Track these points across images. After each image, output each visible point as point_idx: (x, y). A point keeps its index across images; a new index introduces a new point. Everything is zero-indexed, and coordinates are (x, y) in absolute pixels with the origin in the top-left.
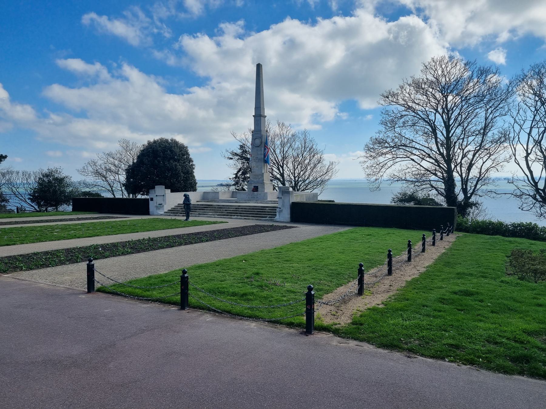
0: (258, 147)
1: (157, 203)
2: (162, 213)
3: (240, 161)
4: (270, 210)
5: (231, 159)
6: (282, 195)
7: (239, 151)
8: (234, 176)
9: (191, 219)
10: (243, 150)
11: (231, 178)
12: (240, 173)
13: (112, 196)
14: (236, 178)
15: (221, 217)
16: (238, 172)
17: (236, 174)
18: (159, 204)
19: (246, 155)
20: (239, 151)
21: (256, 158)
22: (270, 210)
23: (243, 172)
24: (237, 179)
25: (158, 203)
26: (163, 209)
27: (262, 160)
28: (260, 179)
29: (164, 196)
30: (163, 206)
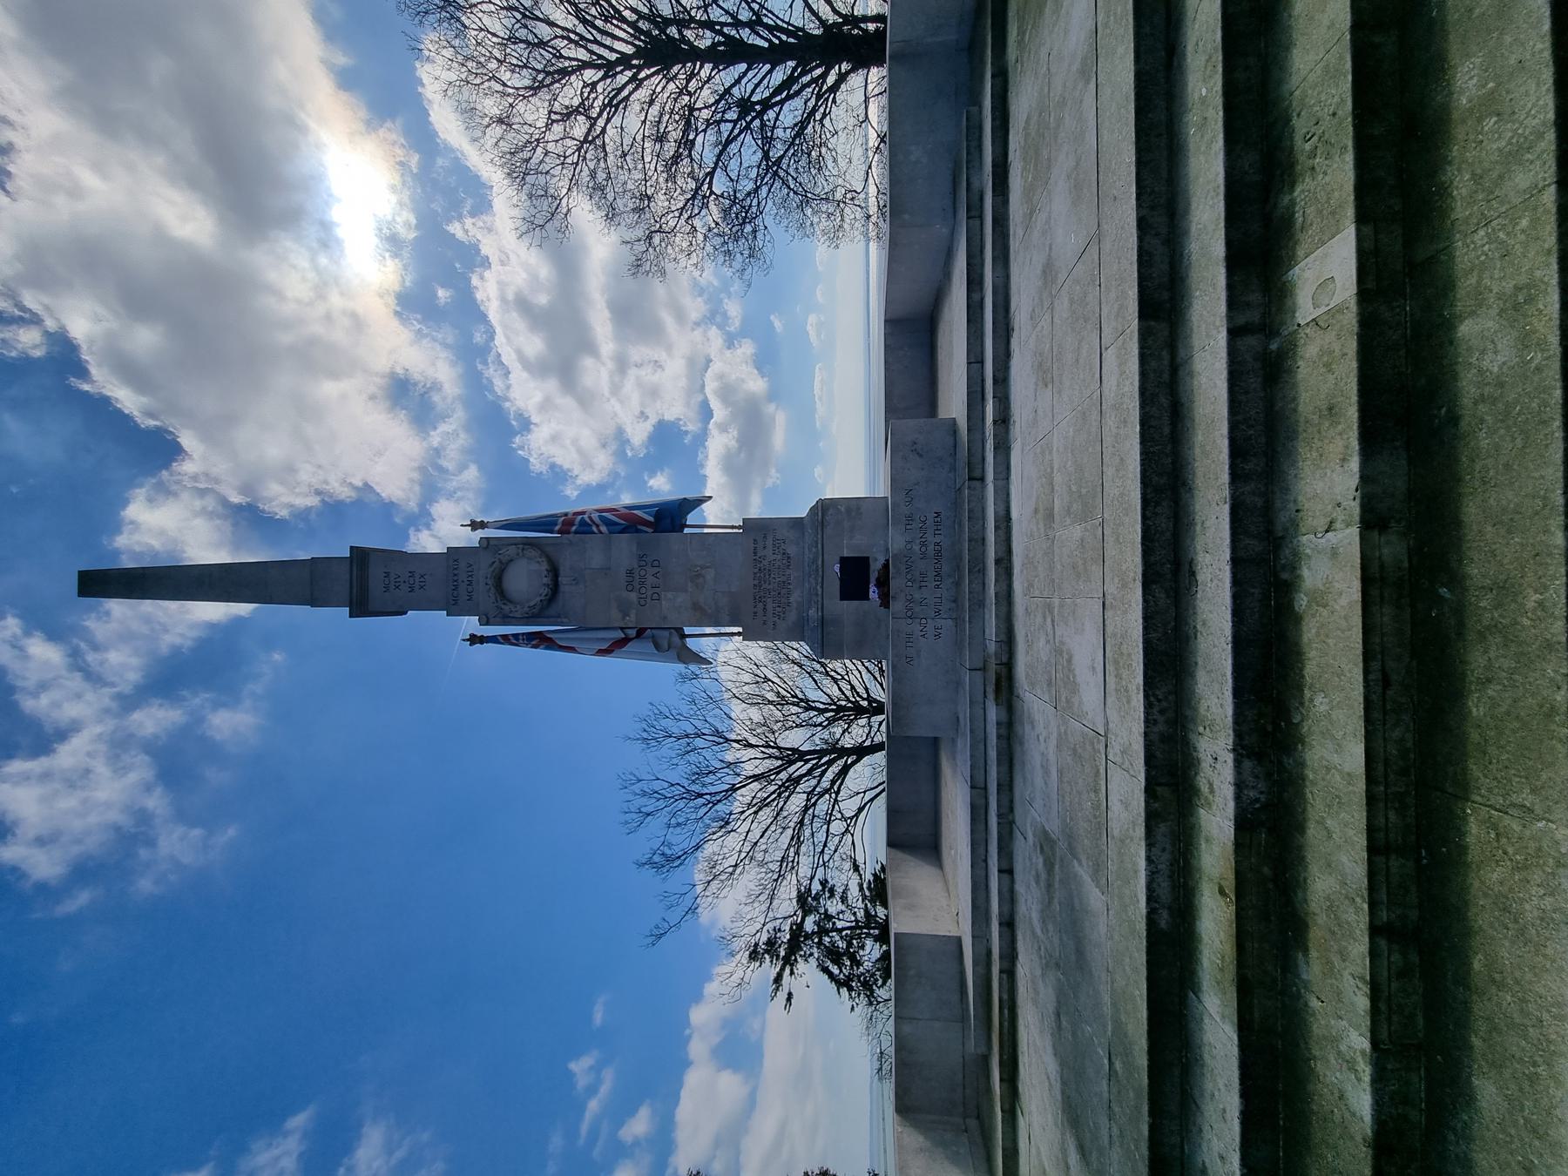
0: (554, 572)
3: (801, 966)
5: (790, 996)
7: (769, 969)
8: (844, 991)
10: (766, 951)
11: (850, 1004)
14: (850, 989)
17: (840, 984)
19: (780, 946)
21: (630, 587)
24: (854, 984)
28: (792, 550)
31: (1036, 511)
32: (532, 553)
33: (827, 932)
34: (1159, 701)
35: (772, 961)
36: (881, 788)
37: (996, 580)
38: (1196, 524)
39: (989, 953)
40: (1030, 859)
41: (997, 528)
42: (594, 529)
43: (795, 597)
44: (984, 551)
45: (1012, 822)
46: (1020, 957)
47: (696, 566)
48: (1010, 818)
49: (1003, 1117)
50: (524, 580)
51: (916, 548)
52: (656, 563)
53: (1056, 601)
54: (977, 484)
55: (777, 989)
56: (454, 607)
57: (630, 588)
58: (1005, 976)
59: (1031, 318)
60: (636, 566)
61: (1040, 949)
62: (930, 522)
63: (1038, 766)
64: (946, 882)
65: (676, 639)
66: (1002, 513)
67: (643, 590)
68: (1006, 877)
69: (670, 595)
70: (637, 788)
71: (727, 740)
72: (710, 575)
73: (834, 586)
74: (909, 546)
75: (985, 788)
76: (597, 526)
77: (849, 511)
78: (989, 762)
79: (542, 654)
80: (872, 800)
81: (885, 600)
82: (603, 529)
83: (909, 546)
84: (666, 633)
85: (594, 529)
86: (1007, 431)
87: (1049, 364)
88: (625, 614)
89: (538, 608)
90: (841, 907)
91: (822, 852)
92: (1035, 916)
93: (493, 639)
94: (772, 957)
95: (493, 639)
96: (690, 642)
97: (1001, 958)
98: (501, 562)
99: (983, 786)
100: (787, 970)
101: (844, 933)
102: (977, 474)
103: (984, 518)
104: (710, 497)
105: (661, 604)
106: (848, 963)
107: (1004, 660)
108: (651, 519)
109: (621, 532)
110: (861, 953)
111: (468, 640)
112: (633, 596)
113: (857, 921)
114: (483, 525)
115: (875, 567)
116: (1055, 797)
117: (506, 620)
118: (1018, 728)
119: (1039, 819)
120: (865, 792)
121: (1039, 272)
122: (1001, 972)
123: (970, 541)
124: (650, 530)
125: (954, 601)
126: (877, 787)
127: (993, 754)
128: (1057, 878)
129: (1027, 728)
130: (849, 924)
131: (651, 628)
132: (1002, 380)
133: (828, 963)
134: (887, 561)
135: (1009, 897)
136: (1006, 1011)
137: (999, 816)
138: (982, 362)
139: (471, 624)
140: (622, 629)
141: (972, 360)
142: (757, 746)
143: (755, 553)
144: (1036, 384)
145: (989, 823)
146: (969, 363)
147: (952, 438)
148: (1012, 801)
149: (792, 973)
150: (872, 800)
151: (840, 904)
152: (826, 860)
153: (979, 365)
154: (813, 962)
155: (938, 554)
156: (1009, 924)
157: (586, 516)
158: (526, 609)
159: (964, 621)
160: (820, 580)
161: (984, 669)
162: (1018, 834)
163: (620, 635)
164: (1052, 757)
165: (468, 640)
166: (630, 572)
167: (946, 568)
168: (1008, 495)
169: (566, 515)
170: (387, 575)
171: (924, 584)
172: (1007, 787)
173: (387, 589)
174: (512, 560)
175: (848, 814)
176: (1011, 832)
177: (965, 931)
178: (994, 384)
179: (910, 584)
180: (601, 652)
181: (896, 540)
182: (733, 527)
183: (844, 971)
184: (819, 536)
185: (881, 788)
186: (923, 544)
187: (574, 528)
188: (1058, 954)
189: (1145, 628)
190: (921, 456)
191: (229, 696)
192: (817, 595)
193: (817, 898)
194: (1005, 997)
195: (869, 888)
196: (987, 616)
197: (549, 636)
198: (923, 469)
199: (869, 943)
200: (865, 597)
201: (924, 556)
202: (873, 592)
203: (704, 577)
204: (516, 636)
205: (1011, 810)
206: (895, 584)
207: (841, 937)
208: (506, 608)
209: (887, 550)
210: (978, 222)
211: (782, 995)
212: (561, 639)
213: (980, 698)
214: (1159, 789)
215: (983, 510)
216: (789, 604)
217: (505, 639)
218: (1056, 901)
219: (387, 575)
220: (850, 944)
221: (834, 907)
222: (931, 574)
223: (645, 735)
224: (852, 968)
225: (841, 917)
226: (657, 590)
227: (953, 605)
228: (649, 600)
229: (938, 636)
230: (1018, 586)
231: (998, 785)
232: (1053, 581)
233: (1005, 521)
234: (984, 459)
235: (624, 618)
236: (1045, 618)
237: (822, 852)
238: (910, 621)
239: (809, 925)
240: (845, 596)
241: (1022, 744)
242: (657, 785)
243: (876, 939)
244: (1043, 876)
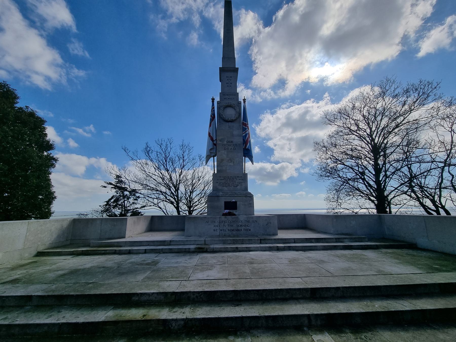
0: (232, 121)
3: (114, 190)
5: (105, 187)
7: (114, 181)
8: (106, 203)
10: (119, 180)
12: (112, 201)
14: (106, 205)
17: (108, 202)
19: (120, 184)
20: (114, 181)
21: (228, 142)
24: (108, 206)
28: (239, 187)
31: (253, 259)
32: (237, 115)
33: (124, 198)
34: (200, 296)
35: (116, 182)
36: (167, 214)
37: (231, 247)
38: (252, 306)
39: (121, 246)
40: (149, 259)
41: (247, 247)
42: (244, 132)
43: (225, 188)
44: (240, 244)
45: (160, 253)
46: (120, 256)
47: (234, 160)
48: (161, 253)
49: (71, 251)
50: (230, 113)
51: (240, 224)
52: (235, 149)
53: (227, 265)
54: (259, 242)
55: (107, 183)
56: (222, 95)
57: (228, 142)
58: (114, 251)
59: (308, 257)
60: (234, 143)
61: (123, 262)
62: (248, 228)
63: (178, 261)
64: (141, 233)
65: (213, 155)
66: (251, 249)
67: (227, 145)
68: (144, 251)
69: (226, 153)
70: (168, 143)
71: (182, 169)
73: (228, 200)
74: (240, 221)
75: (170, 245)
76: (245, 133)
77: (250, 204)
78: (178, 246)
79: (209, 118)
80: (163, 211)
81: (225, 215)
82: (244, 134)
83: (240, 221)
84: (215, 152)
85: (244, 132)
86: (275, 250)
87: (296, 262)
88: (220, 141)
89: (222, 117)
90: (131, 202)
91: (148, 197)
92: (133, 260)
93: (213, 104)
94: (117, 182)
95: (213, 104)
96: (212, 158)
97: (120, 250)
98: (235, 107)
99: (171, 244)
100: (113, 186)
101: (123, 203)
102: (262, 242)
103: (249, 244)
104: (253, 164)
105: (223, 150)
106: (114, 205)
107: (208, 250)
108: (247, 148)
109: (243, 139)
111: (213, 98)
112: (225, 143)
113: (127, 207)
114: (244, 102)
115: (234, 212)
116: (169, 266)
117: (219, 108)
118: (188, 254)
119: (162, 261)
120: (165, 209)
121: (322, 259)
122: (115, 250)
123: (243, 240)
124: (244, 147)
125: (224, 235)
126: (167, 213)
127: (180, 247)
128: (145, 267)
129: (189, 257)
130: (126, 204)
131: (216, 148)
132: (290, 249)
133: (114, 199)
134: (236, 215)
135: (137, 253)
136: (103, 252)
137: (162, 249)
138: (295, 243)
139: (217, 99)
140: (216, 140)
141: (295, 240)
142: (180, 177)
143: (238, 177)
144: (289, 259)
145: (160, 246)
146: (294, 239)
147: (272, 234)
148: (166, 253)
149: (112, 188)
150: (163, 211)
151: (132, 202)
152: (146, 198)
153: (294, 242)
154: (115, 194)
155: (238, 230)
156: (129, 252)
157: (247, 130)
158: (222, 114)
159: (219, 238)
160: (230, 195)
161: (205, 244)
162: (157, 255)
163: (214, 139)
164: (180, 265)
165: (213, 98)
166: (232, 142)
167: (234, 232)
168: (256, 251)
169: (248, 124)
170: (231, 77)
171: (230, 226)
172: (171, 251)
174: (235, 110)
175: (159, 205)
176: (157, 253)
177: (127, 239)
178: (288, 246)
179: (230, 222)
180: (209, 134)
181: (242, 218)
182: (245, 171)
183: (112, 203)
184: (243, 195)
185: (167, 214)
186: (241, 226)
187: (244, 126)
188: (122, 267)
189: (221, 291)
190: (267, 225)
191: (201, 38)
192: (226, 195)
193: (134, 195)
194: (108, 252)
195: (136, 211)
196: (220, 245)
197: (214, 120)
198: (263, 225)
199: (120, 211)
200: (225, 209)
201: (238, 226)
202: (227, 211)
203: (231, 162)
204: (214, 111)
205: (164, 253)
206: (229, 217)
207: (122, 203)
208: (222, 108)
209: (239, 215)
210: (335, 241)
211: (106, 185)
212: (213, 122)
213: (196, 243)
214: (174, 296)
215: (251, 244)
216: (223, 186)
217: (213, 108)
218: (138, 266)
219: (231, 77)
220: (120, 205)
221: (131, 200)
222: (232, 228)
223: (184, 145)
224: (113, 206)
225: (128, 202)
226: (227, 149)
227: (223, 235)
228: (224, 147)
229: (214, 230)
230: (230, 254)
231: (171, 249)
232: (233, 264)
233: (248, 250)
234: (266, 243)
235: (219, 140)
236: (221, 262)
237: (148, 197)
238: (219, 222)
239: (126, 193)
240: (225, 202)
241: (184, 255)
242: (169, 149)
243: (121, 213)
244: (145, 262)
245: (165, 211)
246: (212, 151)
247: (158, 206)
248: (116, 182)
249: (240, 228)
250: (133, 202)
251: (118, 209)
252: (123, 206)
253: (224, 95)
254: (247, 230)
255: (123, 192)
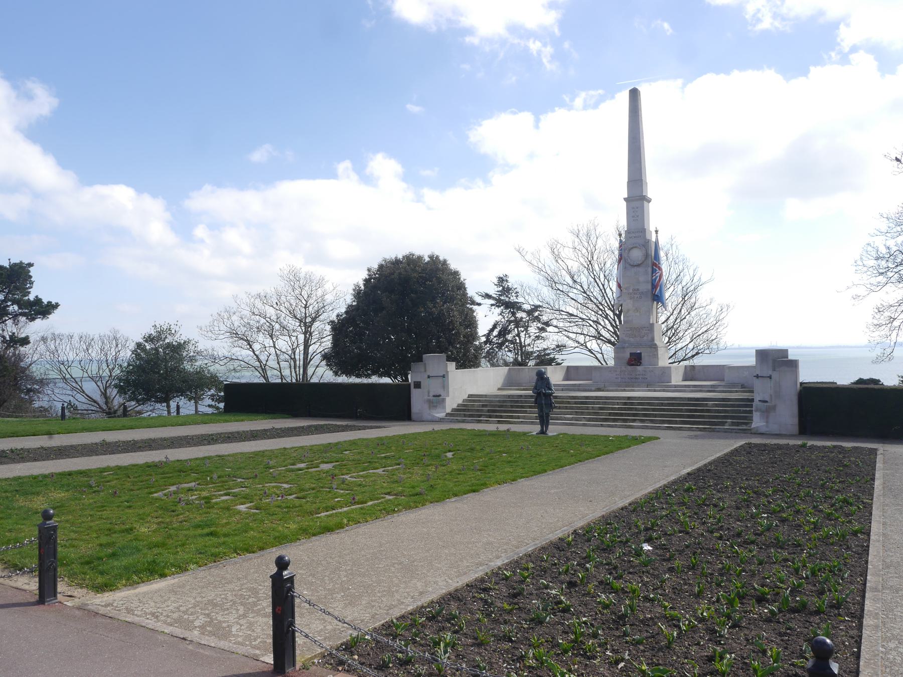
0: (638, 265)
1: (429, 393)
2: (442, 415)
3: (498, 310)
4: (717, 405)
6: (774, 370)
7: (493, 290)
9: (553, 430)
12: (495, 333)
13: (262, 381)
15: (602, 425)
16: (492, 330)
18: (434, 396)
19: (507, 296)
20: (493, 290)
21: (634, 290)
22: (717, 405)
23: (500, 332)
24: (488, 345)
25: (432, 394)
26: (444, 408)
27: (650, 295)
28: (645, 338)
29: (444, 376)
30: (444, 400)
33: (517, 327)
35: (498, 291)
36: (604, 364)
43: (631, 339)
55: (483, 296)
69: (632, 302)
72: (638, 314)
77: (655, 355)
80: (597, 358)
82: (654, 277)
88: (626, 289)
91: (566, 331)
94: (500, 291)
101: (517, 338)
110: (506, 349)
112: (631, 291)
113: (525, 346)
120: (601, 353)
126: (605, 361)
130: (523, 340)
149: (492, 305)
150: (597, 358)
154: (499, 318)
166: (638, 290)
173: (633, 208)
175: (588, 345)
183: (495, 339)
185: (603, 362)
207: (514, 337)
219: (637, 208)
221: (533, 329)
224: (497, 343)
225: (527, 336)
237: (566, 331)
239: (520, 315)
240: (631, 354)
243: (516, 359)
245: (599, 356)
246: (619, 299)
247: (587, 348)
248: (498, 291)
249: (638, 377)
250: (537, 334)
251: (508, 351)
252: (520, 348)
253: (629, 233)
254: (644, 378)
255: (514, 314)
